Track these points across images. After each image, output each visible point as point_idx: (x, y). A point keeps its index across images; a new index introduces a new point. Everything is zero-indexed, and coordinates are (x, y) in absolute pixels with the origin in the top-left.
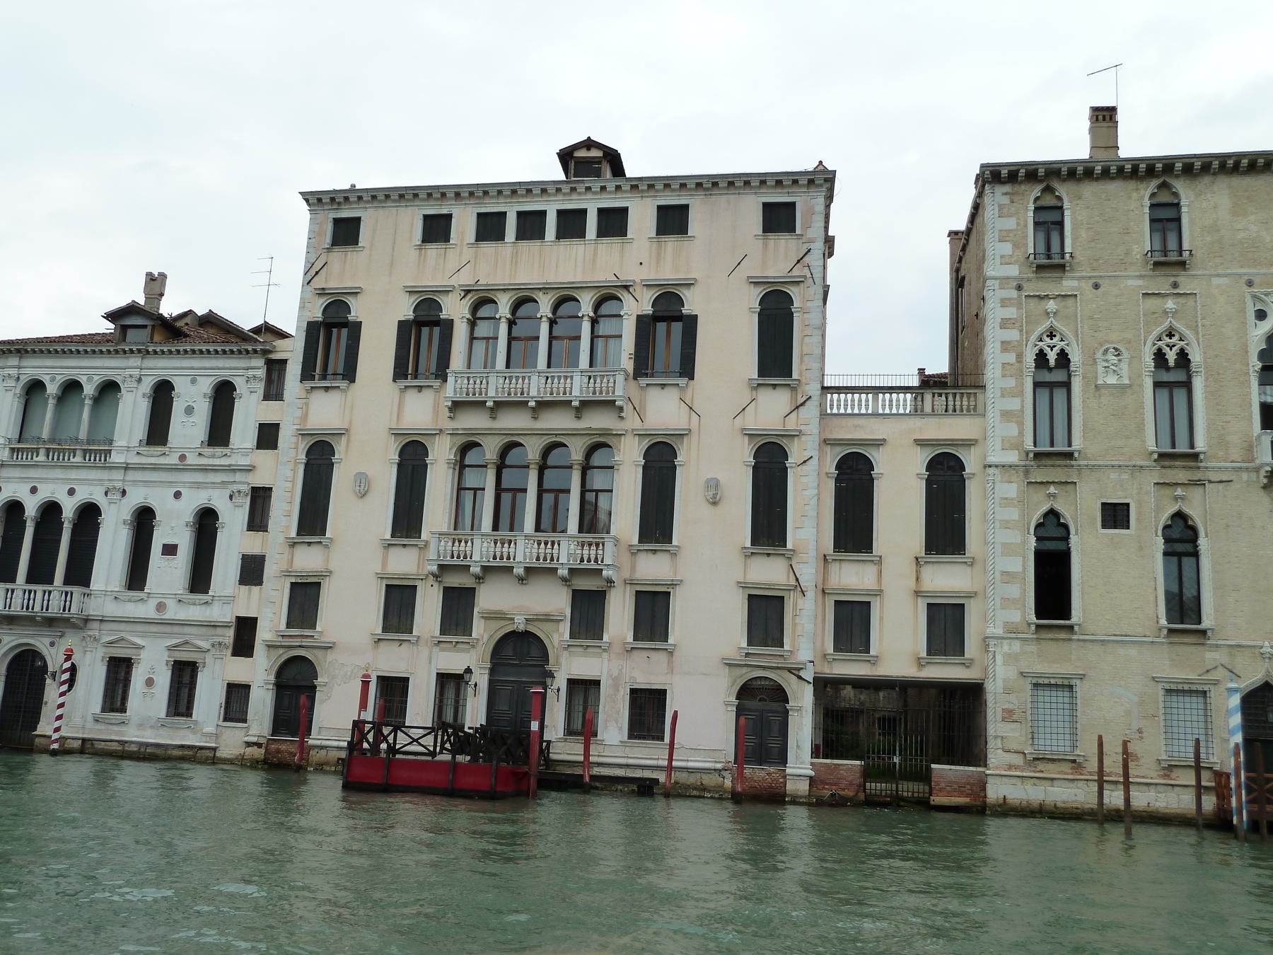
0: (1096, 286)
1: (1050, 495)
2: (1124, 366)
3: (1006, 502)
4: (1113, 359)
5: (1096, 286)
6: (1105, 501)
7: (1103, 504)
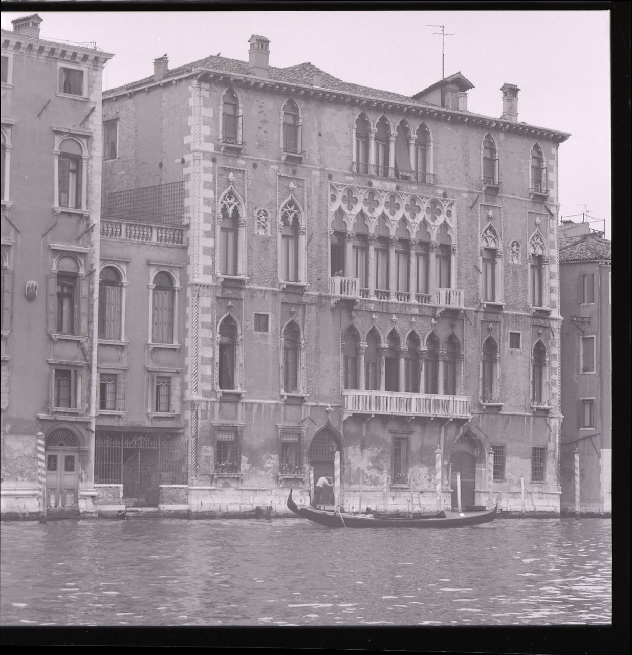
1: (229, 307)
2: (268, 223)
3: (205, 310)
5: (255, 166)
6: (256, 312)
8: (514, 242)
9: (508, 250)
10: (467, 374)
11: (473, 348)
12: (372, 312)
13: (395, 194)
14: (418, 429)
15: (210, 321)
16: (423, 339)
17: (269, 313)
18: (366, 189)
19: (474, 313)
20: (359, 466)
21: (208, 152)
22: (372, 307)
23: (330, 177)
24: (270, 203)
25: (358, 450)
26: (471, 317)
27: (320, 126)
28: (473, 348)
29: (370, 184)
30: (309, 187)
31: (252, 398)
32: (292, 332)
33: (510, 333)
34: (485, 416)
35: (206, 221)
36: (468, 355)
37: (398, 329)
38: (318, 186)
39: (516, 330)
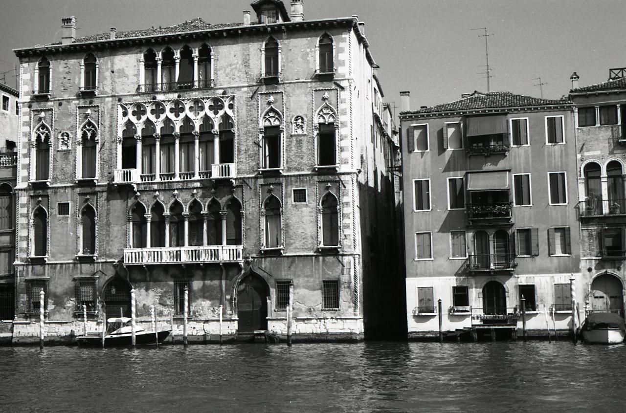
0: (60, 104)
4: (66, 138)
5: (60, 104)
7: (59, 204)
8: (298, 117)
9: (290, 125)
10: (248, 227)
11: (253, 207)
12: (155, 191)
13: (177, 100)
14: (199, 273)
15: (26, 212)
16: (205, 205)
17: (69, 202)
18: (151, 102)
19: (253, 180)
20: (144, 303)
21: (26, 102)
22: (156, 187)
23: (120, 100)
24: (72, 127)
25: (143, 290)
26: (251, 183)
27: (112, 66)
28: (253, 207)
29: (154, 98)
30: (103, 110)
31: (56, 260)
32: (88, 213)
33: (294, 190)
34: (268, 259)
35: (24, 147)
36: (248, 212)
37: (180, 200)
38: (110, 108)
39: (300, 187)
